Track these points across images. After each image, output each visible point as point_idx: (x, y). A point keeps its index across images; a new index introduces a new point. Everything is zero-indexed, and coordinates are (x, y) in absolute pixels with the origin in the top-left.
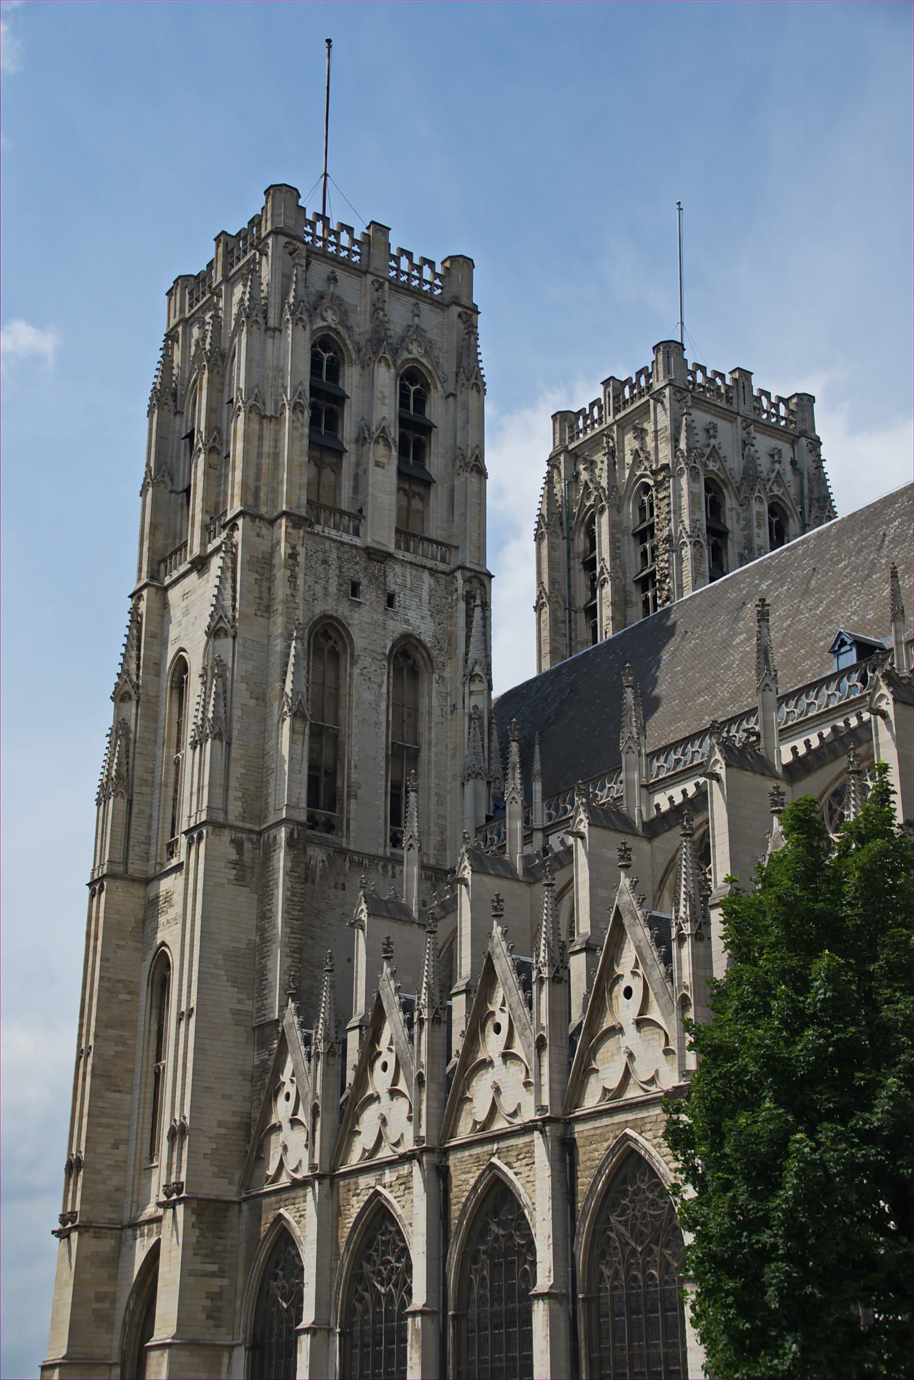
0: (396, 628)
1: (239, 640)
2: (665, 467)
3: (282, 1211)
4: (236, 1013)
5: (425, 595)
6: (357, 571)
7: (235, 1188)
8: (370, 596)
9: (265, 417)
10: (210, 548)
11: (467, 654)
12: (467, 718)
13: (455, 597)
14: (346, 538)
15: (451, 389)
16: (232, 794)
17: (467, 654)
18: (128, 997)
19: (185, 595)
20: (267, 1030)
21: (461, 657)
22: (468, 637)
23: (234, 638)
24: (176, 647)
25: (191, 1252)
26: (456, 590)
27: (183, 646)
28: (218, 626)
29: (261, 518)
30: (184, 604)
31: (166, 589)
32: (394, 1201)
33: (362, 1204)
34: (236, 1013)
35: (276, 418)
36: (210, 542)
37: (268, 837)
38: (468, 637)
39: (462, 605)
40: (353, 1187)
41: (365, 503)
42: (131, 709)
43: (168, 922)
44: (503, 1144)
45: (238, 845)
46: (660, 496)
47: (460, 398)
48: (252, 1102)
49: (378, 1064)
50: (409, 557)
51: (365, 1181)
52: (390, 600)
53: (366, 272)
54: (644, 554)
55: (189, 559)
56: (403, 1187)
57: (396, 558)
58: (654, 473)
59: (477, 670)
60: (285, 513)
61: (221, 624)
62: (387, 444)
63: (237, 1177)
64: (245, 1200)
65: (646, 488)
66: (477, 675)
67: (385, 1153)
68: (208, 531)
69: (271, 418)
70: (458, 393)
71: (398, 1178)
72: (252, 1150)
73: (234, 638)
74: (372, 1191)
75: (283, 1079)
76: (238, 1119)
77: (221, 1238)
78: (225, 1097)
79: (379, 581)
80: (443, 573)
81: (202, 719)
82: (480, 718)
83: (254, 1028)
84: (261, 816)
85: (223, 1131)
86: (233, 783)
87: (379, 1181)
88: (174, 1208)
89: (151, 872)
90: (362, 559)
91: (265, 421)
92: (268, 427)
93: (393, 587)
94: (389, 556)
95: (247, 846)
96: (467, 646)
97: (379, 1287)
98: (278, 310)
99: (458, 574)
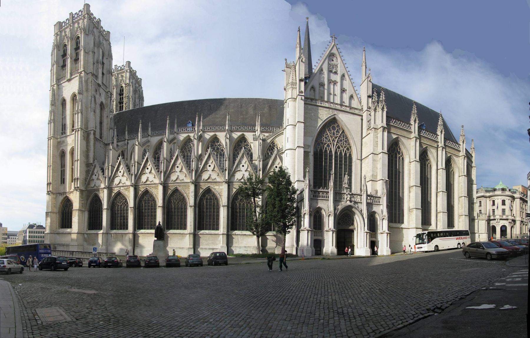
8: (98, 93)
34: (84, 161)
45: (84, 132)
50: (103, 87)
52: (100, 94)
79: (99, 90)
86: (83, 122)
90: (97, 85)
93: (101, 92)
94: (100, 86)
95: (85, 133)
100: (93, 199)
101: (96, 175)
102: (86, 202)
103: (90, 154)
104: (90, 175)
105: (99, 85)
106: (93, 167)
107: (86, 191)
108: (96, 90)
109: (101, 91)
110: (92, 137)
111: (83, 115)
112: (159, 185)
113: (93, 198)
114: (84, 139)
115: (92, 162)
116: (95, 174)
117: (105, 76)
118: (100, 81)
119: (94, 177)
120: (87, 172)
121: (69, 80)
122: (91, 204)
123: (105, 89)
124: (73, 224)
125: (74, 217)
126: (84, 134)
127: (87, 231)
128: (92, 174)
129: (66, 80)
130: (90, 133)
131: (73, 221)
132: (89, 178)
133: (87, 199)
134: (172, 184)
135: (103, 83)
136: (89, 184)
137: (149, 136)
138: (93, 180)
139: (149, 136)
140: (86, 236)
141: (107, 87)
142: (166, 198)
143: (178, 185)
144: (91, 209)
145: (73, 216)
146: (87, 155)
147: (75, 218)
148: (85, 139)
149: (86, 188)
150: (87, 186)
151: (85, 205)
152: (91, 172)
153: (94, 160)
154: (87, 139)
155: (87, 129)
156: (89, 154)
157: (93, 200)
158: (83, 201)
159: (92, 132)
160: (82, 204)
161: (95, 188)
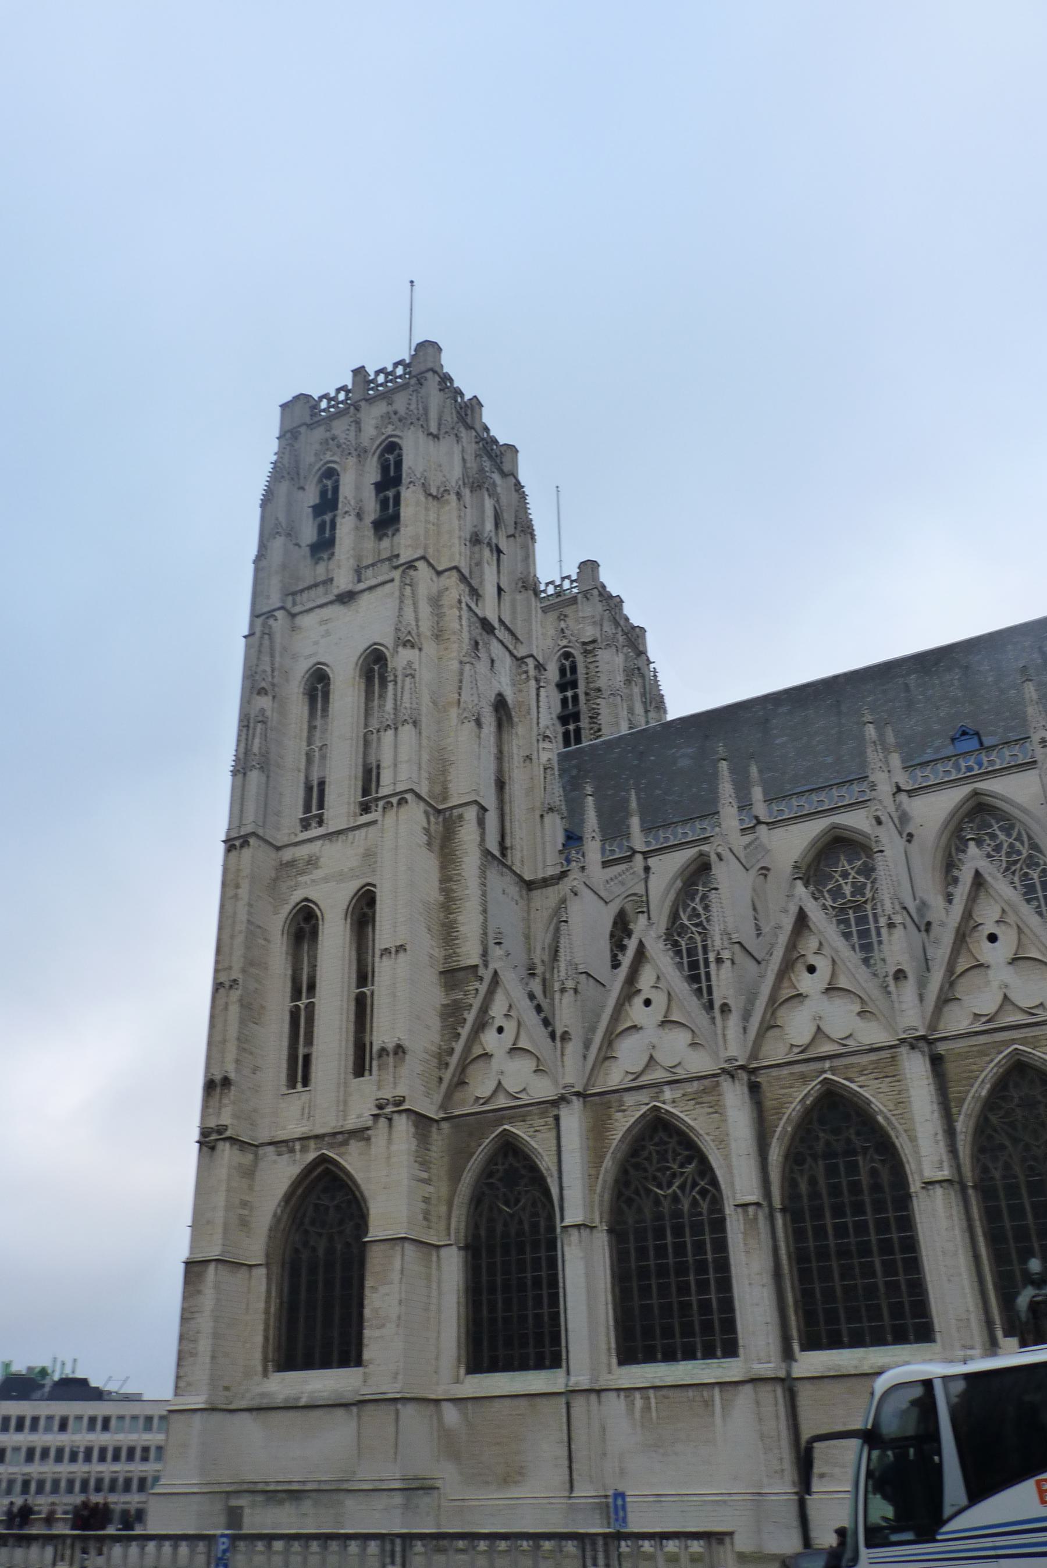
0: (496, 688)
1: (423, 653)
2: (594, 641)
3: (506, 1127)
4: (431, 956)
5: (507, 668)
6: (478, 631)
7: (434, 1108)
8: (482, 654)
9: (430, 495)
10: (362, 586)
11: (538, 718)
12: (542, 768)
13: (524, 676)
14: (473, 606)
15: (511, 531)
16: (422, 772)
17: (538, 718)
18: (263, 942)
19: (324, 622)
20: (461, 975)
21: (535, 721)
22: (538, 707)
23: (420, 649)
24: (313, 660)
25: (412, 1159)
26: (526, 672)
27: (322, 660)
28: (407, 638)
29: (434, 568)
30: (324, 627)
31: (293, 616)
32: (681, 1115)
33: (633, 1120)
34: (431, 956)
35: (438, 499)
36: (359, 581)
37: (451, 815)
38: (538, 707)
39: (533, 683)
40: (615, 1104)
41: (481, 583)
42: (264, 702)
43: (313, 881)
44: (837, 1062)
46: (589, 660)
47: (519, 539)
48: (442, 1036)
49: (638, 1001)
51: (629, 1099)
52: (493, 661)
53: (472, 428)
54: (564, 702)
55: (336, 592)
56: (693, 1102)
57: (495, 635)
58: (584, 644)
59: (548, 733)
60: (456, 568)
61: (409, 638)
62: (491, 551)
63: (438, 1097)
64: (444, 1119)
65: (567, 655)
66: (548, 737)
67: (658, 1075)
68: (359, 573)
69: (435, 497)
70: (517, 535)
71: (684, 1095)
72: (453, 1075)
73: (420, 649)
74: (645, 1108)
75: (492, 1013)
76: (434, 1049)
77: (428, 1150)
78: (428, 1027)
79: (487, 644)
80: (515, 657)
81: (395, 709)
82: (552, 769)
83: (441, 973)
84: (445, 796)
85: (428, 1057)
87: (656, 1098)
88: (390, 1120)
89: (285, 840)
91: (430, 498)
92: (433, 504)
93: (494, 656)
95: (432, 819)
96: (538, 712)
97: (659, 1191)
98: (436, 424)
99: (531, 662)
100: (487, 1173)
101: (500, 1030)
102: (444, 1191)
103: (461, 918)
104: (465, 1032)
105: (486, 626)
106: (483, 988)
107: (445, 1125)
108: (477, 643)
109: (496, 649)
110: (468, 834)
111: (424, 734)
112: (904, 1050)
113: (491, 1161)
114: (429, 844)
115: (474, 960)
116: (497, 1024)
117: (506, 598)
118: (489, 610)
119: (490, 1040)
120: (452, 1014)
121: (347, 598)
122: (477, 1200)
123: (511, 647)
124: (367, 1333)
125: (374, 1289)
126: (429, 822)
127: (457, 1381)
128: (481, 1026)
129: (332, 597)
130: (461, 817)
131: (367, 1312)
132: (459, 1047)
133: (455, 1176)
134: (983, 1039)
135: (501, 621)
136: (460, 1082)
137: (759, 822)
138: (487, 1056)
139: (759, 822)
140: (451, 1415)
141: (517, 639)
142: (959, 1126)
143: (1024, 1041)
144: (483, 1233)
145: (369, 1283)
146: (443, 925)
147: (383, 1290)
148: (437, 843)
149: (443, 1107)
150: (448, 1096)
151: (443, 1209)
152: (471, 1017)
153: (485, 954)
154: (442, 847)
155: (445, 799)
156: (455, 921)
157: (491, 1175)
158: (427, 1182)
159: (471, 814)
160: (426, 1200)
161: (502, 1102)
